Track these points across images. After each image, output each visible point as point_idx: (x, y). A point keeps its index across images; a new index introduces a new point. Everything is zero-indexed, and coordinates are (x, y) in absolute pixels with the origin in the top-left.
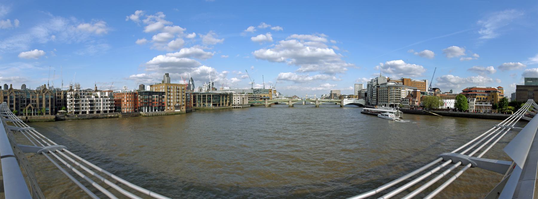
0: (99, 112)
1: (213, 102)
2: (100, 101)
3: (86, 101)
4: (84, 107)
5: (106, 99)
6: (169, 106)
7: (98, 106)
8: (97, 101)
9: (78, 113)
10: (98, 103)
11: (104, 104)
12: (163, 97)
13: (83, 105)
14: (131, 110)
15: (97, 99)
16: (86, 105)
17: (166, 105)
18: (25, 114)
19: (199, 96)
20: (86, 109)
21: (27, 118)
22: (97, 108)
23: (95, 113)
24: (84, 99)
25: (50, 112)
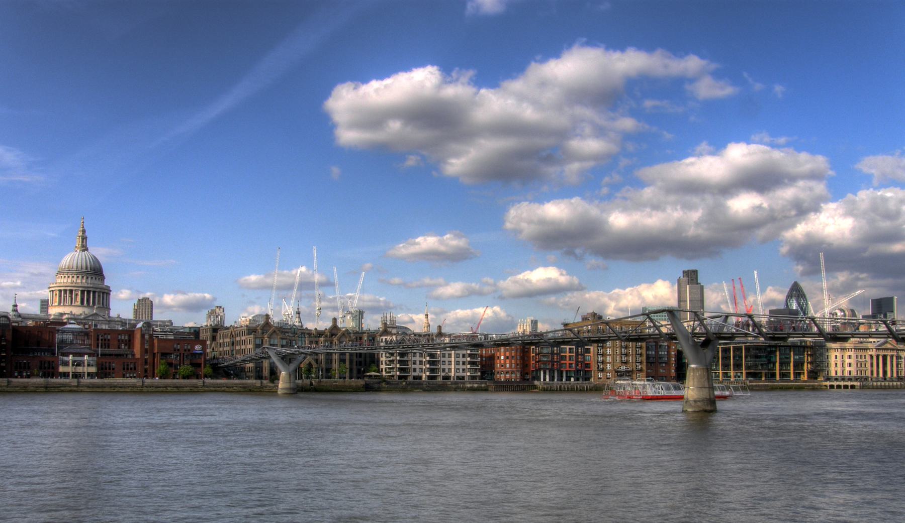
0: (447, 378)
1: (748, 368)
2: (450, 355)
4: (417, 366)
6: (602, 370)
7: (446, 367)
8: (444, 356)
9: (405, 377)
10: (446, 359)
11: (457, 363)
12: (588, 351)
13: (415, 363)
17: (594, 367)
22: (444, 370)
23: (440, 379)
25: (347, 374)
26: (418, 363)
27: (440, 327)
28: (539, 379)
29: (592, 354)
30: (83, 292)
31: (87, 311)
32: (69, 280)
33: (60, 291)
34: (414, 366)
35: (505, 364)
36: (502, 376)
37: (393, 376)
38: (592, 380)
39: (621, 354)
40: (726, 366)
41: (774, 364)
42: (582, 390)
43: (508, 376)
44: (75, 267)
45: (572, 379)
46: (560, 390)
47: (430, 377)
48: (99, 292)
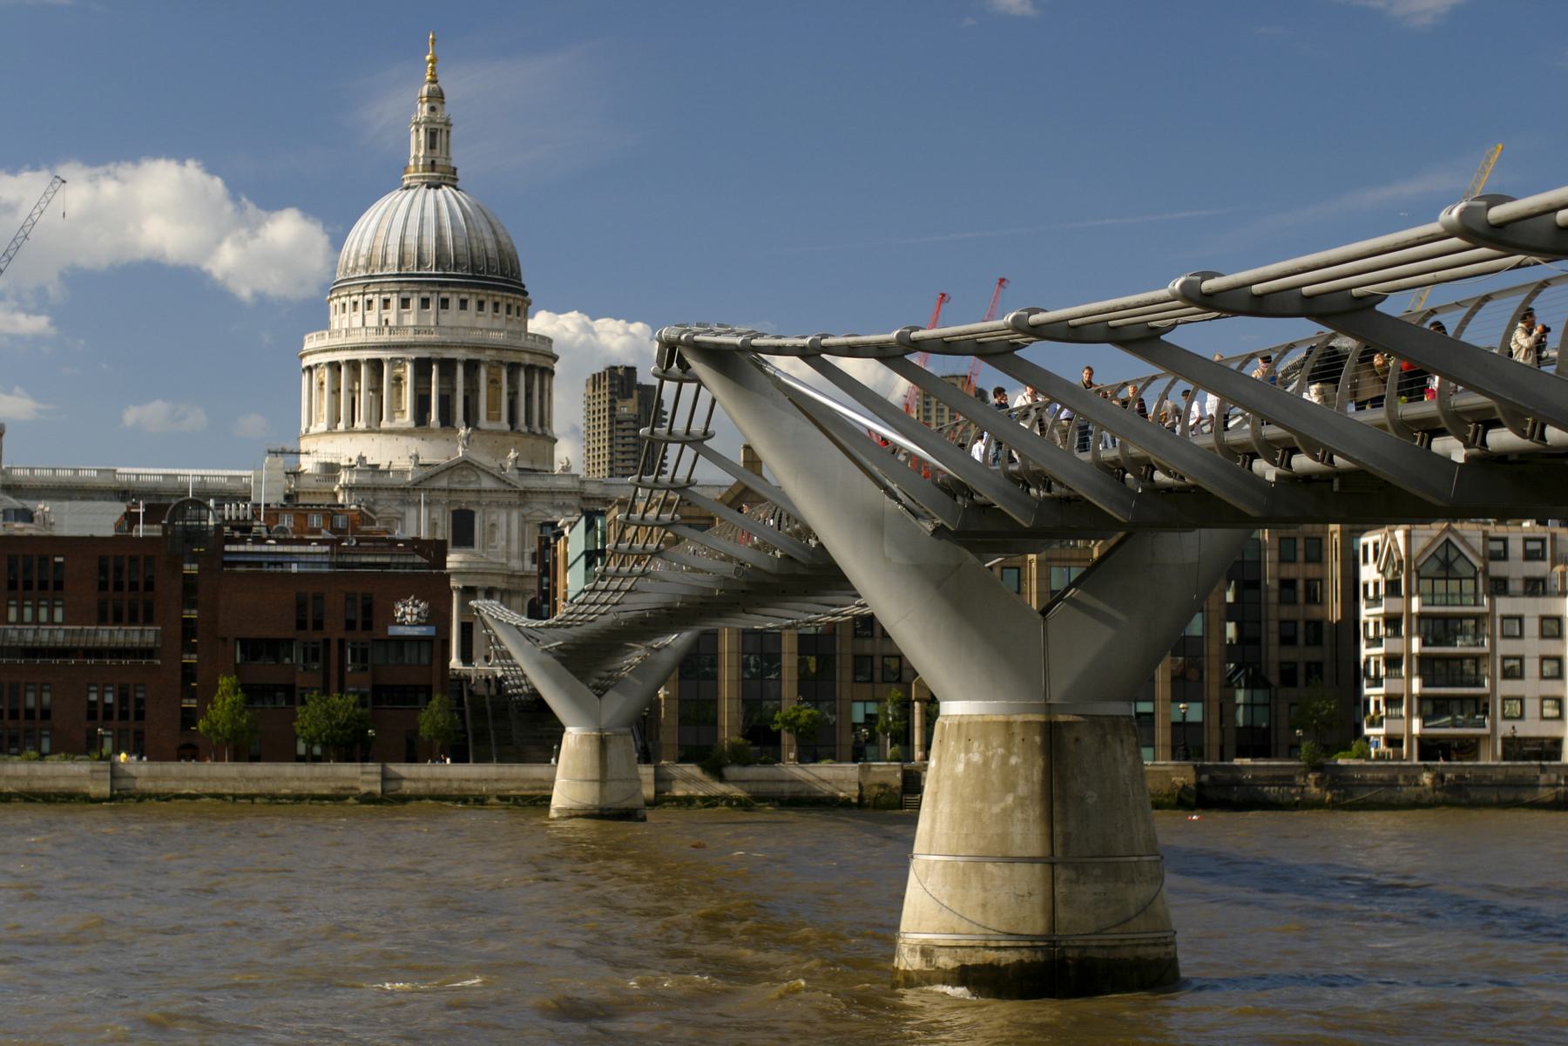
26: (1532, 667)
30: (422, 368)
32: (372, 320)
33: (335, 367)
34: (1506, 687)
48: (496, 365)
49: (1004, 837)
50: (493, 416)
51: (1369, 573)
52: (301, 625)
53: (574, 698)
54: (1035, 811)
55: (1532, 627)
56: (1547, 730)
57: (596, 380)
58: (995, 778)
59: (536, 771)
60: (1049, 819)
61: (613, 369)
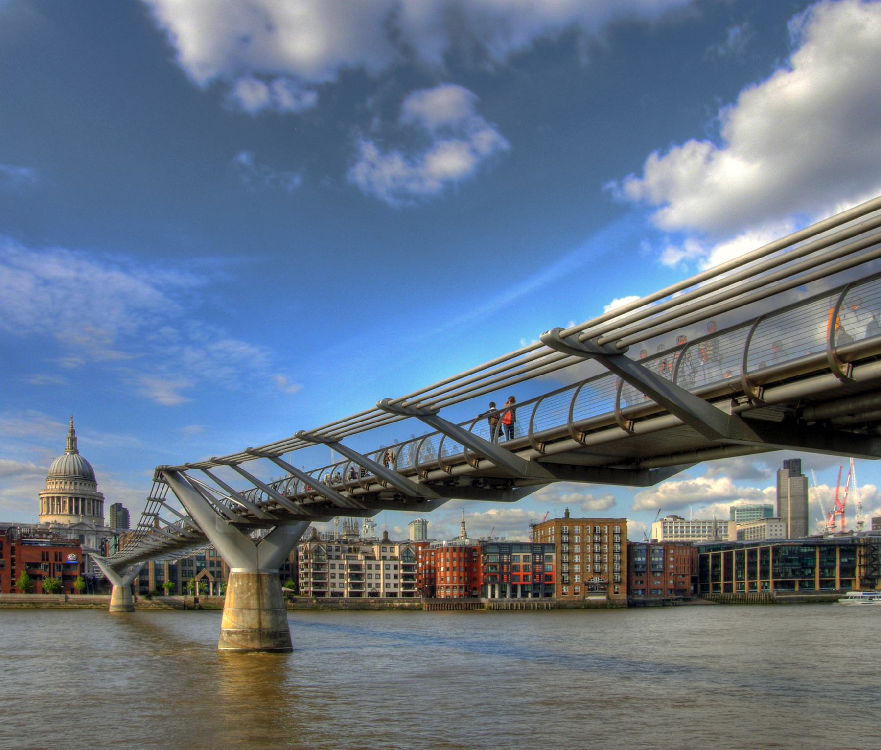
1: (775, 575)
2: (378, 567)
3: (341, 566)
4: (337, 580)
5: (392, 563)
6: (568, 584)
7: (373, 581)
8: (370, 567)
10: (373, 571)
11: (387, 576)
13: (333, 577)
14: (456, 592)
15: (369, 562)
16: (341, 576)
17: (557, 580)
18: (194, 590)
19: (738, 553)
20: (342, 585)
21: (196, 600)
22: (370, 585)
24: (337, 562)
26: (337, 576)
27: (386, 533)
28: (486, 596)
29: (554, 563)
30: (71, 499)
31: (74, 520)
33: (48, 498)
34: (332, 580)
35: (446, 577)
36: (443, 592)
37: (307, 592)
38: (555, 595)
39: (594, 562)
40: (752, 574)
41: (813, 568)
42: (540, 609)
43: (449, 592)
44: (63, 472)
45: (530, 595)
46: (512, 609)
47: (352, 594)
49: (248, 603)
50: (89, 512)
51: (301, 554)
52: (43, 559)
53: (115, 578)
54: (255, 597)
55: (337, 567)
56: (340, 590)
57: (112, 506)
58: (245, 588)
59: (105, 597)
60: (259, 599)
61: (116, 504)
